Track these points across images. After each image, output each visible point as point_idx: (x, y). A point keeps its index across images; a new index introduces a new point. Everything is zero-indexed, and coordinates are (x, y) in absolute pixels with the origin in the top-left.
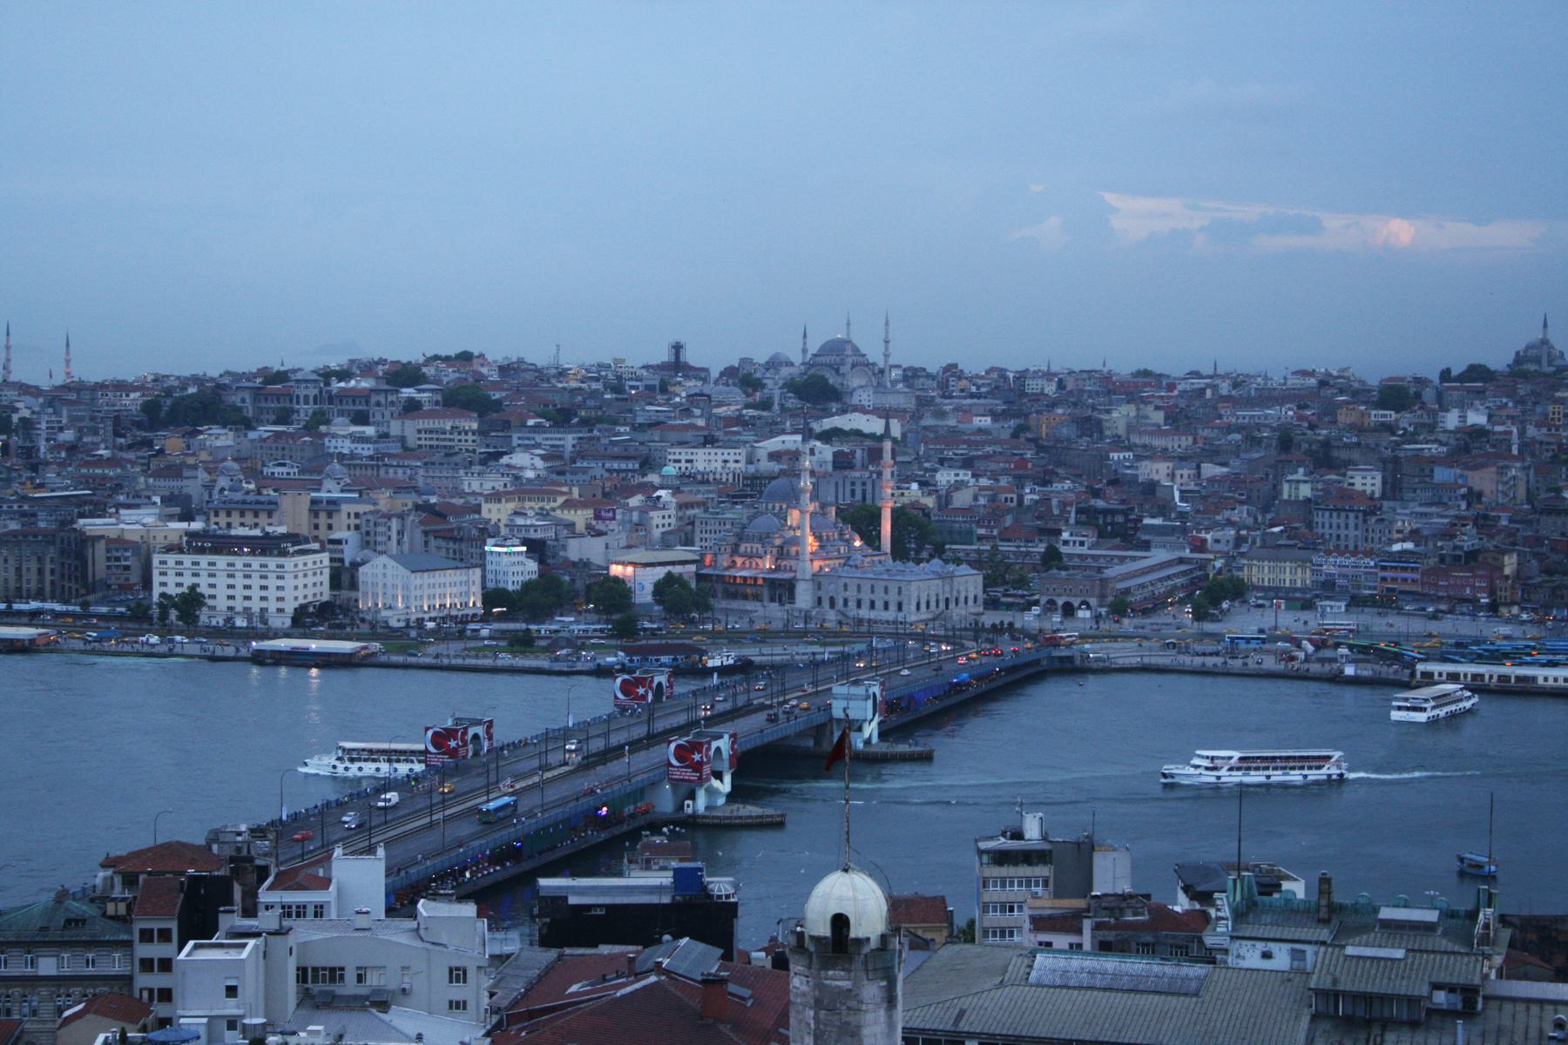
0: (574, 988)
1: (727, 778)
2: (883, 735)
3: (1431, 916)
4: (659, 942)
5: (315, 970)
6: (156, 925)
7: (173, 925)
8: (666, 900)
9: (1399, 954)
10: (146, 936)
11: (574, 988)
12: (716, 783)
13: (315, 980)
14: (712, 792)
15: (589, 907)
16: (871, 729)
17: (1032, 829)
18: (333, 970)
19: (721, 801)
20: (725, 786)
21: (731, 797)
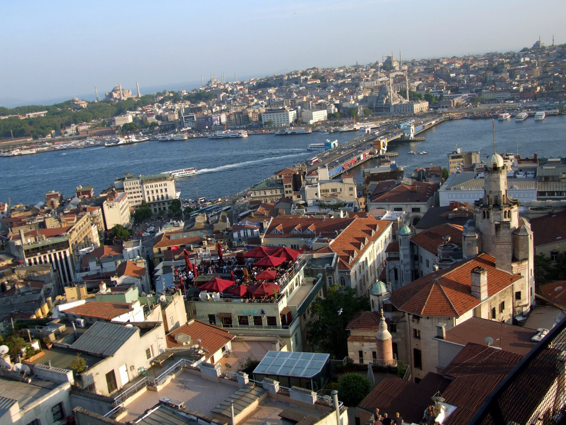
0: (384, 188)
1: (386, 147)
2: (414, 136)
3: (559, 160)
4: (399, 178)
5: (323, 190)
6: (288, 184)
7: (291, 184)
8: (389, 171)
9: (554, 167)
10: (286, 186)
11: (384, 188)
12: (384, 149)
13: (323, 192)
14: (383, 151)
15: (374, 174)
16: (412, 136)
17: (459, 151)
18: (326, 190)
19: (385, 152)
20: (385, 149)
21: (387, 151)
